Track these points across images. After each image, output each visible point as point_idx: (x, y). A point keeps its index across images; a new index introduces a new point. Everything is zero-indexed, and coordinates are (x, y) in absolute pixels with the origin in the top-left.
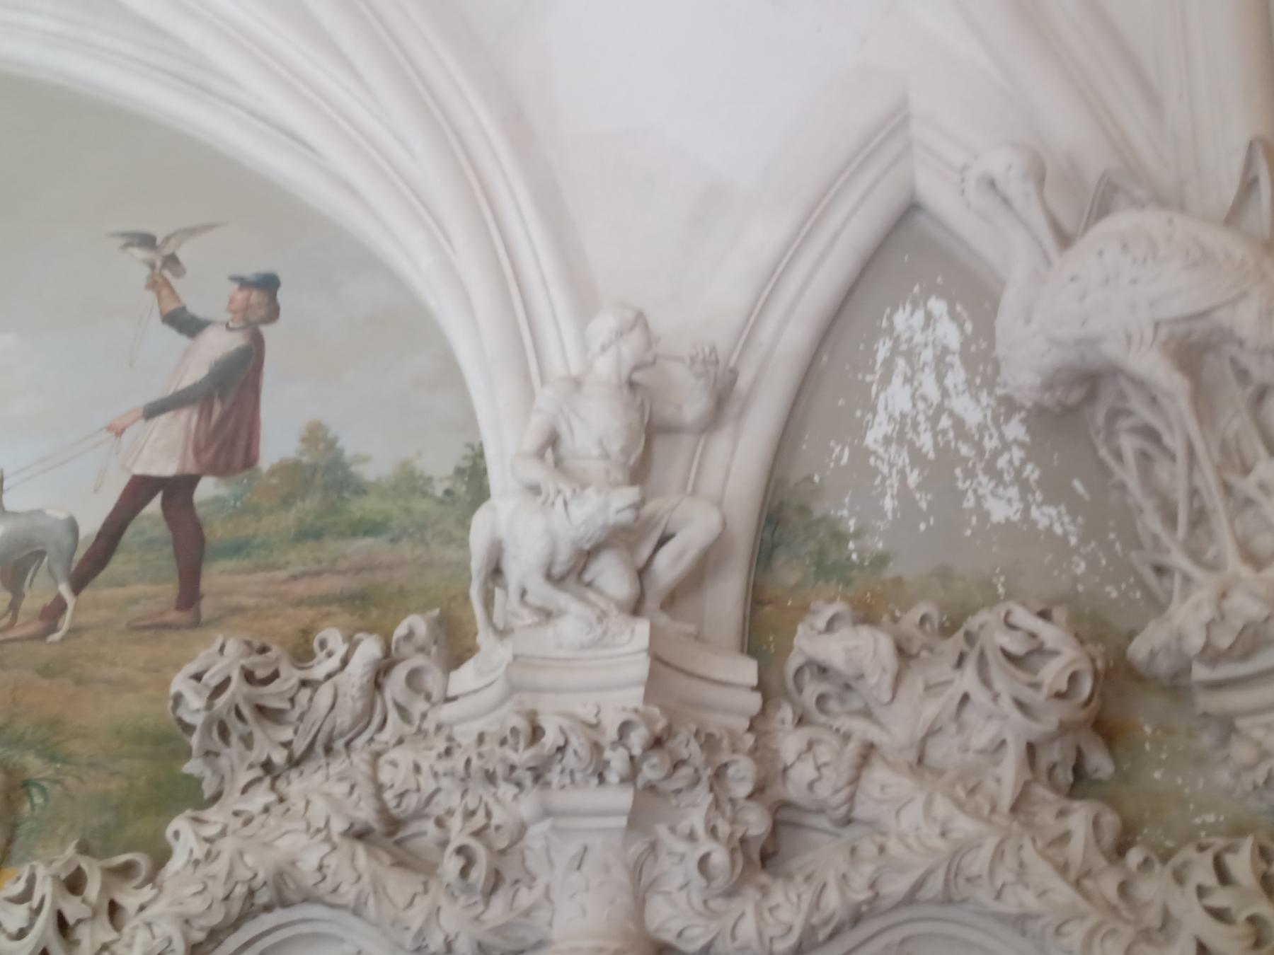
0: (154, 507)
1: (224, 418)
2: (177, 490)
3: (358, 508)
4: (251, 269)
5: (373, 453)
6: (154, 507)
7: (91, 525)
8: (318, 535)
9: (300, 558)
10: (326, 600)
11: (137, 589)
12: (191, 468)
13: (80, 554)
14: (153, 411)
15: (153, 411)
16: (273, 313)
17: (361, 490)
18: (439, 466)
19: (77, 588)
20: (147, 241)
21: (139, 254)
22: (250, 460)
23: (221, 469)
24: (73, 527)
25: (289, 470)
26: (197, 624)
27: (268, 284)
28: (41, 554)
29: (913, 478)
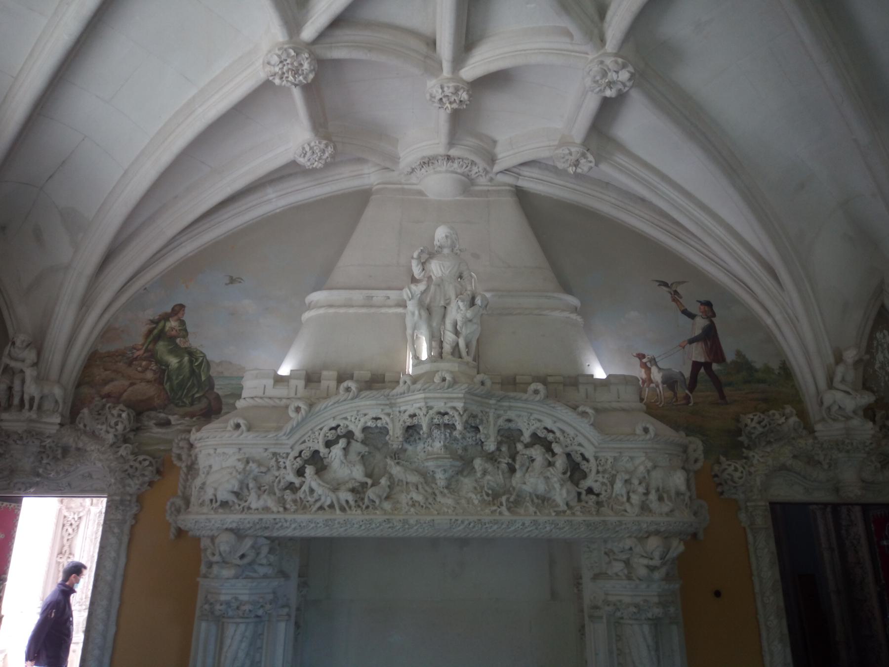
0: (702, 370)
2: (707, 366)
4: (703, 299)
5: (757, 360)
6: (702, 370)
7: (687, 374)
12: (708, 360)
13: (688, 382)
14: (691, 341)
15: (691, 341)
16: (714, 315)
17: (756, 371)
18: (775, 365)
19: (691, 392)
20: (665, 284)
23: (718, 362)
24: (682, 375)
27: (708, 304)
28: (676, 382)
29: (887, 378)
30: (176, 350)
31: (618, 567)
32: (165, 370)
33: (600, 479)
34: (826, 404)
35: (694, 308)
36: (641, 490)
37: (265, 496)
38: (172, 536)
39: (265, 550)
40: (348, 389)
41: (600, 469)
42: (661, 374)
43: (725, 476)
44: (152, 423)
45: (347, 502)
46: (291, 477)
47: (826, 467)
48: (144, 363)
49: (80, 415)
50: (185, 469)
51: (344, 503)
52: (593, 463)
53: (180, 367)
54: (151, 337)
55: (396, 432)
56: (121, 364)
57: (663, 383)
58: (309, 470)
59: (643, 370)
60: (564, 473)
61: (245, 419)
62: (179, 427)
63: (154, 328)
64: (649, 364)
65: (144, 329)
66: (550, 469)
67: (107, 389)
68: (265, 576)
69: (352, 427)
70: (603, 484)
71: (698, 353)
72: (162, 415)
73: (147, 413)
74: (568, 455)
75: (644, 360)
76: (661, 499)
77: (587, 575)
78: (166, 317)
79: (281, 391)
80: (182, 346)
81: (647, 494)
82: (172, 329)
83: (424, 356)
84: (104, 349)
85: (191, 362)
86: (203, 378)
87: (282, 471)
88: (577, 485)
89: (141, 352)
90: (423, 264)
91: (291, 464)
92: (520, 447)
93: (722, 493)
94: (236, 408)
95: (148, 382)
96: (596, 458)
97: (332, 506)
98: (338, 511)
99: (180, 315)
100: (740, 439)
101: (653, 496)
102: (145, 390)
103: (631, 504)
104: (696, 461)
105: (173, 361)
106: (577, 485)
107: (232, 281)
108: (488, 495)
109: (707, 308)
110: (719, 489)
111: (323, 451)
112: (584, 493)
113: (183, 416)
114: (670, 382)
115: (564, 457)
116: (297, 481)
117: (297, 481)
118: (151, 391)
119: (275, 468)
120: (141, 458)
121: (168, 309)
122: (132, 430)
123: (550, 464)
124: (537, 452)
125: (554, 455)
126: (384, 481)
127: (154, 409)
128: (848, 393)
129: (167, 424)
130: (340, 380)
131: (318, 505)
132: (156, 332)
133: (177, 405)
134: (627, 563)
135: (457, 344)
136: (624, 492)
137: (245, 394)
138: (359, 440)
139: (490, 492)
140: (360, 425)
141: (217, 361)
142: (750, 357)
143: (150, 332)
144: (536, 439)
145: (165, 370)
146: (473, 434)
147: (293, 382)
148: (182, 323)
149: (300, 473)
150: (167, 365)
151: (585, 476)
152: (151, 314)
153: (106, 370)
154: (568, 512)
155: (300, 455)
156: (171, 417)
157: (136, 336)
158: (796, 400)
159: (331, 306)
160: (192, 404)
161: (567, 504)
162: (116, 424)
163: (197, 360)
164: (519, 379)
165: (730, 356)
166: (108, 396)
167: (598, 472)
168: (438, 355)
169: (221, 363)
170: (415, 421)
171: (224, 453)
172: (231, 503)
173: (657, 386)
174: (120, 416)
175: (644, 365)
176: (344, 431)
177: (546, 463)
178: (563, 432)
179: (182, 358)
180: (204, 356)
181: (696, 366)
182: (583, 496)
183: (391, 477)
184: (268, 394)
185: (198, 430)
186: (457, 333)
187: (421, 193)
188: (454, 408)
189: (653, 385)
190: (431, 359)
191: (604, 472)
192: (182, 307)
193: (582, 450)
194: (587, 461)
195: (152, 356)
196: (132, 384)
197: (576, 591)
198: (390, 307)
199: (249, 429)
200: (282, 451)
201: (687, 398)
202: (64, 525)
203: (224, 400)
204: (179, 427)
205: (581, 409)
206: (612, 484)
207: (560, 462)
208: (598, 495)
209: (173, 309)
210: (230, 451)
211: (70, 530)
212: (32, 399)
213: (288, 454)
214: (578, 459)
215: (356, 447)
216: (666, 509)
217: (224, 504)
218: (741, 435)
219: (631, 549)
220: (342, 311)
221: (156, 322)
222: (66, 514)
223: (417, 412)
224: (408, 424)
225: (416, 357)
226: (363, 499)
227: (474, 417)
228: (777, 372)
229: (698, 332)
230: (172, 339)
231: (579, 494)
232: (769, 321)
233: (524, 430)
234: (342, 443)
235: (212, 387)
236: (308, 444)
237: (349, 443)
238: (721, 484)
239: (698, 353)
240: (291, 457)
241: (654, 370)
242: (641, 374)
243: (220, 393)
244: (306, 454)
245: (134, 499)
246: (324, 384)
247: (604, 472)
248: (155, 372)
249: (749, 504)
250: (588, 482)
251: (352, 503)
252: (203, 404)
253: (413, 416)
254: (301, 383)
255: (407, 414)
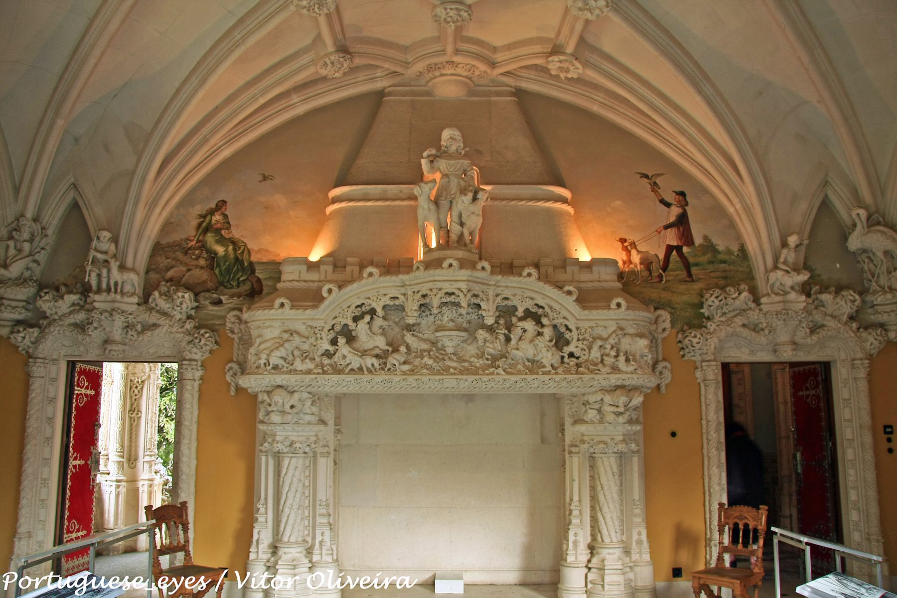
0: (674, 253)
1: (684, 231)
2: (679, 249)
3: (721, 257)
4: (677, 190)
6: (674, 253)
7: (661, 256)
8: (713, 263)
9: (710, 268)
10: (718, 277)
11: (678, 272)
12: (680, 244)
14: (666, 227)
15: (666, 227)
16: (687, 204)
17: (719, 253)
18: (735, 248)
20: (646, 176)
21: (646, 180)
22: (693, 243)
23: (688, 245)
25: (700, 245)
26: (693, 281)
27: (682, 194)
30: (221, 241)
31: (592, 414)
32: (214, 258)
33: (581, 346)
34: (771, 282)
35: (670, 198)
36: (613, 353)
37: (307, 361)
38: (232, 393)
39: (309, 403)
40: (371, 274)
41: (581, 337)
42: (639, 256)
43: (686, 341)
44: (207, 303)
45: (373, 365)
46: (327, 346)
47: (767, 332)
48: (197, 252)
49: (152, 297)
50: (237, 340)
51: (370, 366)
52: (575, 333)
53: (226, 256)
54: (201, 229)
55: (412, 307)
56: (178, 253)
57: (641, 264)
58: (342, 341)
59: (624, 253)
60: (551, 341)
61: (288, 298)
62: (229, 305)
63: (203, 222)
64: (629, 248)
65: (195, 223)
66: (539, 337)
67: (170, 274)
68: (309, 423)
69: (374, 305)
70: (583, 349)
71: (672, 238)
72: (215, 295)
73: (202, 294)
74: (555, 327)
75: (626, 244)
76: (627, 360)
77: (568, 421)
78: (212, 212)
79: (314, 276)
80: (227, 236)
81: (616, 357)
82: (217, 222)
83: (434, 245)
84: (164, 242)
85: (235, 250)
86: (246, 264)
87: (319, 341)
88: (561, 350)
89: (194, 242)
90: (432, 162)
91: (327, 337)
92: (514, 320)
93: (683, 356)
94: (277, 290)
95: (202, 268)
96: (578, 329)
97: (361, 369)
98: (366, 372)
99: (223, 210)
100: (702, 311)
101: (622, 358)
102: (200, 275)
103: (604, 365)
104: (664, 330)
105: (220, 250)
106: (561, 350)
107: (265, 178)
108: (487, 359)
109: (681, 198)
110: (681, 353)
111: (352, 325)
112: (566, 356)
113: (232, 296)
114: (647, 263)
115: (551, 329)
116: (331, 349)
117: (331, 349)
118: (204, 275)
119: (314, 338)
120: (202, 331)
121: (214, 206)
122: (192, 309)
123: (540, 334)
124: (529, 325)
125: (543, 326)
126: (403, 349)
127: (208, 291)
128: (787, 272)
129: (219, 302)
130: (362, 267)
131: (349, 368)
132: (204, 225)
133: (225, 287)
134: (599, 411)
135: (462, 234)
136: (598, 355)
137: (284, 277)
138: (381, 315)
139: (489, 357)
140: (382, 304)
141: (256, 249)
142: (715, 240)
143: (200, 225)
144: (529, 315)
145: (214, 258)
146: (476, 310)
147: (323, 268)
148: (225, 216)
149: (334, 342)
150: (216, 254)
151: (567, 343)
152: (199, 209)
153: (167, 258)
154: (553, 371)
155: (333, 328)
156: (222, 297)
157: (190, 229)
158: (749, 277)
159: (351, 200)
160: (238, 286)
161: (552, 366)
162: (181, 303)
163: (240, 248)
164: (516, 262)
165: (698, 240)
166: (171, 280)
167: (578, 340)
168: (446, 244)
169: (259, 251)
170: (427, 300)
171: (271, 326)
172: (280, 366)
173: (636, 266)
174: (183, 297)
175: (625, 249)
176: (368, 308)
177: (536, 333)
178: (551, 308)
179: (227, 247)
180: (246, 245)
181: (670, 249)
182: (566, 360)
183: (408, 347)
184: (302, 278)
185: (249, 308)
186: (462, 224)
187: (429, 94)
188: (459, 289)
189: (632, 266)
190: (440, 247)
191: (584, 340)
192: (224, 202)
193: (566, 322)
194: (570, 331)
195: (203, 246)
196: (189, 270)
197: (560, 435)
198: (403, 200)
199: (292, 307)
200: (319, 324)
201: (660, 276)
202: (131, 388)
203: (264, 283)
204: (229, 305)
205: (567, 288)
206: (590, 348)
207: (548, 332)
208: (578, 358)
209: (217, 205)
210: (277, 324)
211: (136, 391)
212: (116, 284)
213: (323, 328)
214: (563, 329)
215: (378, 322)
216: (631, 369)
217: (276, 367)
218: (702, 308)
219: (602, 400)
220: (360, 204)
221: (204, 217)
222: (132, 378)
223: (429, 293)
224: (421, 302)
225: (426, 245)
226: (385, 364)
227: (476, 296)
228: (736, 254)
229: (672, 219)
230: (218, 231)
231: (563, 357)
232: (732, 210)
233: (519, 307)
234: (367, 318)
235: (253, 272)
236: (338, 320)
237: (372, 318)
238: (683, 348)
239: (672, 238)
240: (326, 330)
241: (634, 252)
242: (620, 256)
243: (260, 276)
244: (338, 328)
245: (199, 364)
246: (349, 269)
247: (584, 340)
248: (207, 260)
249: (704, 364)
250: (571, 348)
251: (377, 365)
252: (246, 287)
253: (424, 296)
254: (330, 268)
255: (420, 294)
